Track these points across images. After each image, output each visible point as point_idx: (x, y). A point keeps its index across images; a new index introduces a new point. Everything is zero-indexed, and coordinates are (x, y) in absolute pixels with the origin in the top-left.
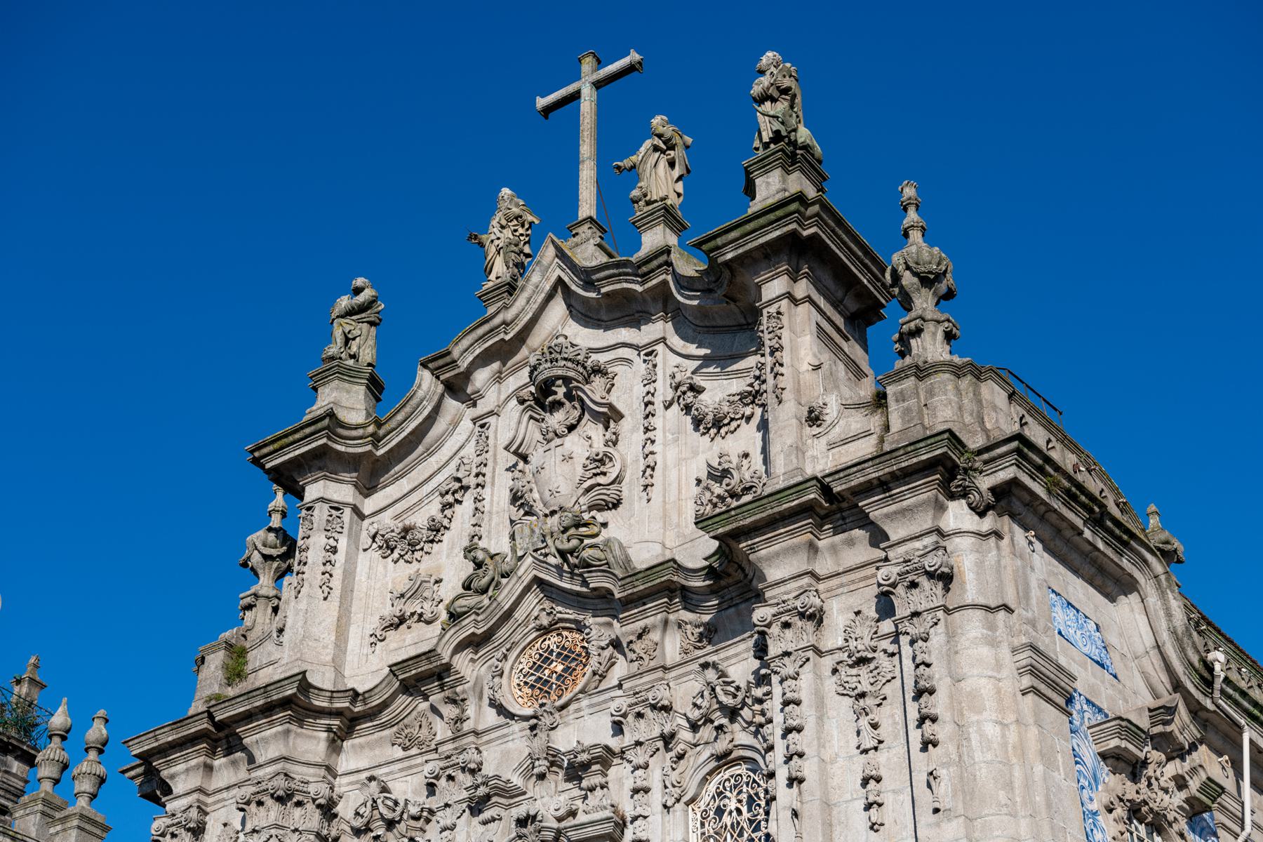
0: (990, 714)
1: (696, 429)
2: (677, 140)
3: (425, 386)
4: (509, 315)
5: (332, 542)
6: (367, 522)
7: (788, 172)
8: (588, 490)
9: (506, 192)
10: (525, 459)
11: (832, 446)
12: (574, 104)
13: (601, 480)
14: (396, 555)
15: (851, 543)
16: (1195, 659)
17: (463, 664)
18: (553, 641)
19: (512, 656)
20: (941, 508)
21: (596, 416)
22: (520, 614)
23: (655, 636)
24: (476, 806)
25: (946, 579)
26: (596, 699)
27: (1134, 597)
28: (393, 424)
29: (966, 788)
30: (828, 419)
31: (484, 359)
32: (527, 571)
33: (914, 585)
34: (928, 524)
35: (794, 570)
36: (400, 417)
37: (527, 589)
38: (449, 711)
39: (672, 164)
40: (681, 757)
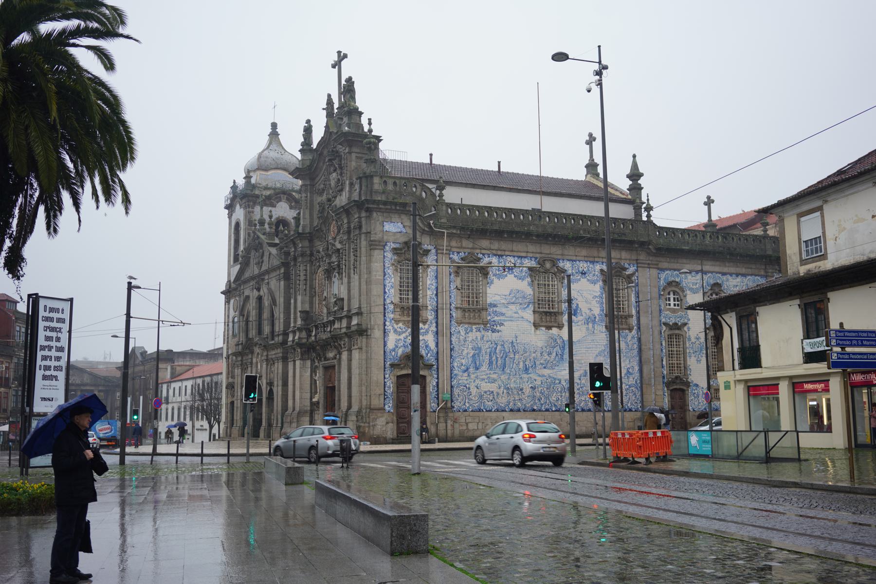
25: (360, 227)
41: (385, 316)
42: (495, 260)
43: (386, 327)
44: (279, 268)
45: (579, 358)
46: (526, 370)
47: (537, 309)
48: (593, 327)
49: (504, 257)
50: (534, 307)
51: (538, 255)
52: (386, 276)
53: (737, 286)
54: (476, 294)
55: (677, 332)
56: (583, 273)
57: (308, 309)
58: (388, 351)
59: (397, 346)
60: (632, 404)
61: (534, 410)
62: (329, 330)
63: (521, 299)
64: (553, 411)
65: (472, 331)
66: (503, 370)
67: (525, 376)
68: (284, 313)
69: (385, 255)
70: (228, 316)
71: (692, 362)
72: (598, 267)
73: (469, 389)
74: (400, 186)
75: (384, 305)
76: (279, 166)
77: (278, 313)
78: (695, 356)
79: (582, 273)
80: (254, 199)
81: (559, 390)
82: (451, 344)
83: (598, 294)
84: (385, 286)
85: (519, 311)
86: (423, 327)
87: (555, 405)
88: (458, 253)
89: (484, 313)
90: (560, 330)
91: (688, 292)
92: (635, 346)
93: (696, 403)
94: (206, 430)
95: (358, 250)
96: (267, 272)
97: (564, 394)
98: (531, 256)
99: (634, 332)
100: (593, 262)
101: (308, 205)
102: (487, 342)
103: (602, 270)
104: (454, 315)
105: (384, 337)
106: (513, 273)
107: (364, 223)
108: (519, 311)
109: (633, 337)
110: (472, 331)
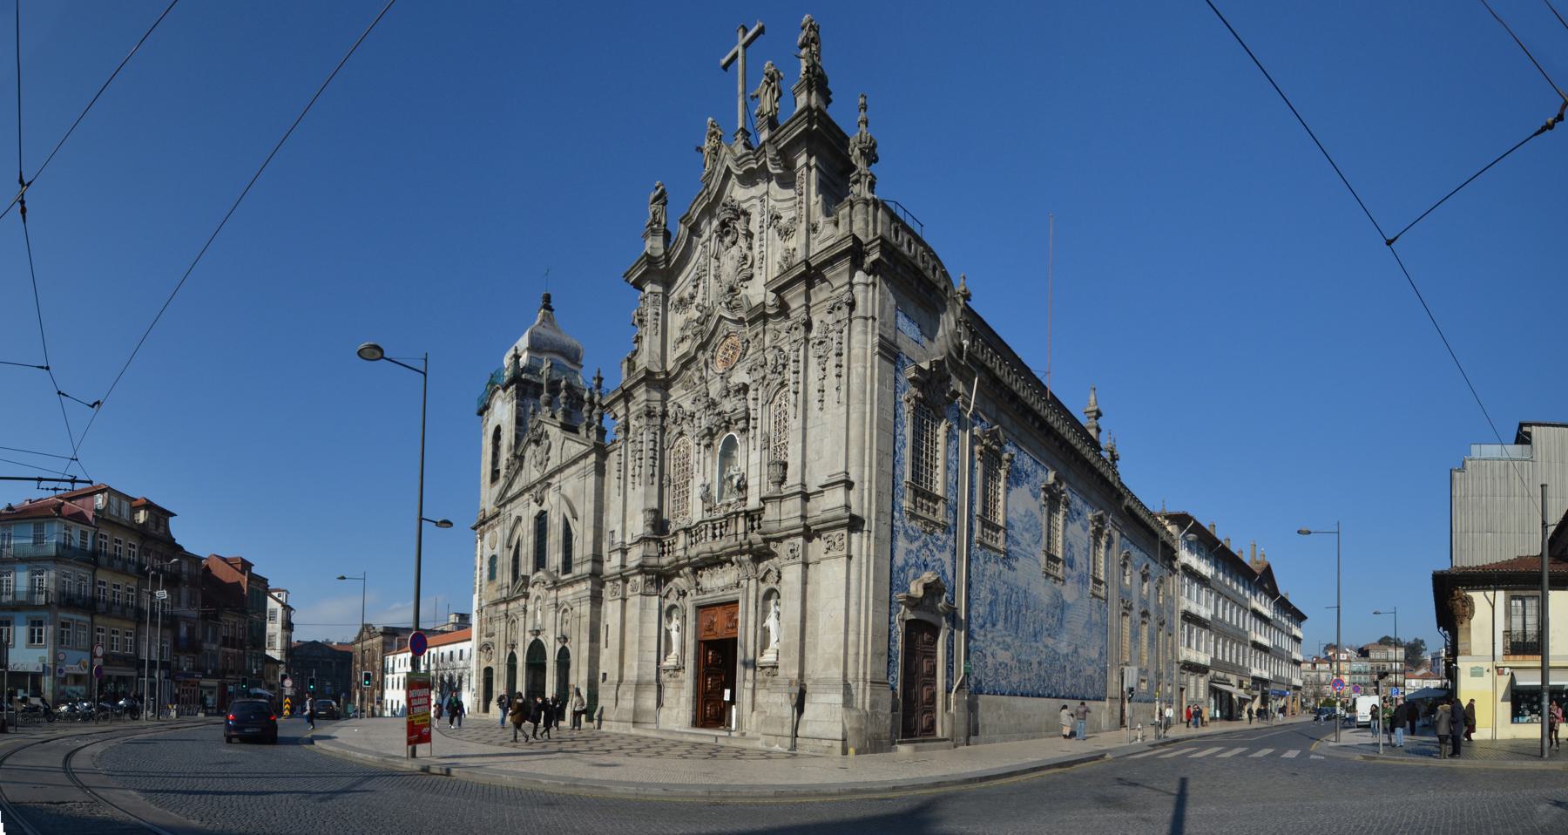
41: (893, 499)
46: (1035, 636)
58: (895, 569)
59: (907, 563)
61: (1039, 696)
62: (733, 531)
66: (1017, 630)
67: (1034, 644)
73: (985, 656)
83: (1086, 546)
85: (1033, 545)
86: (941, 536)
105: (892, 541)
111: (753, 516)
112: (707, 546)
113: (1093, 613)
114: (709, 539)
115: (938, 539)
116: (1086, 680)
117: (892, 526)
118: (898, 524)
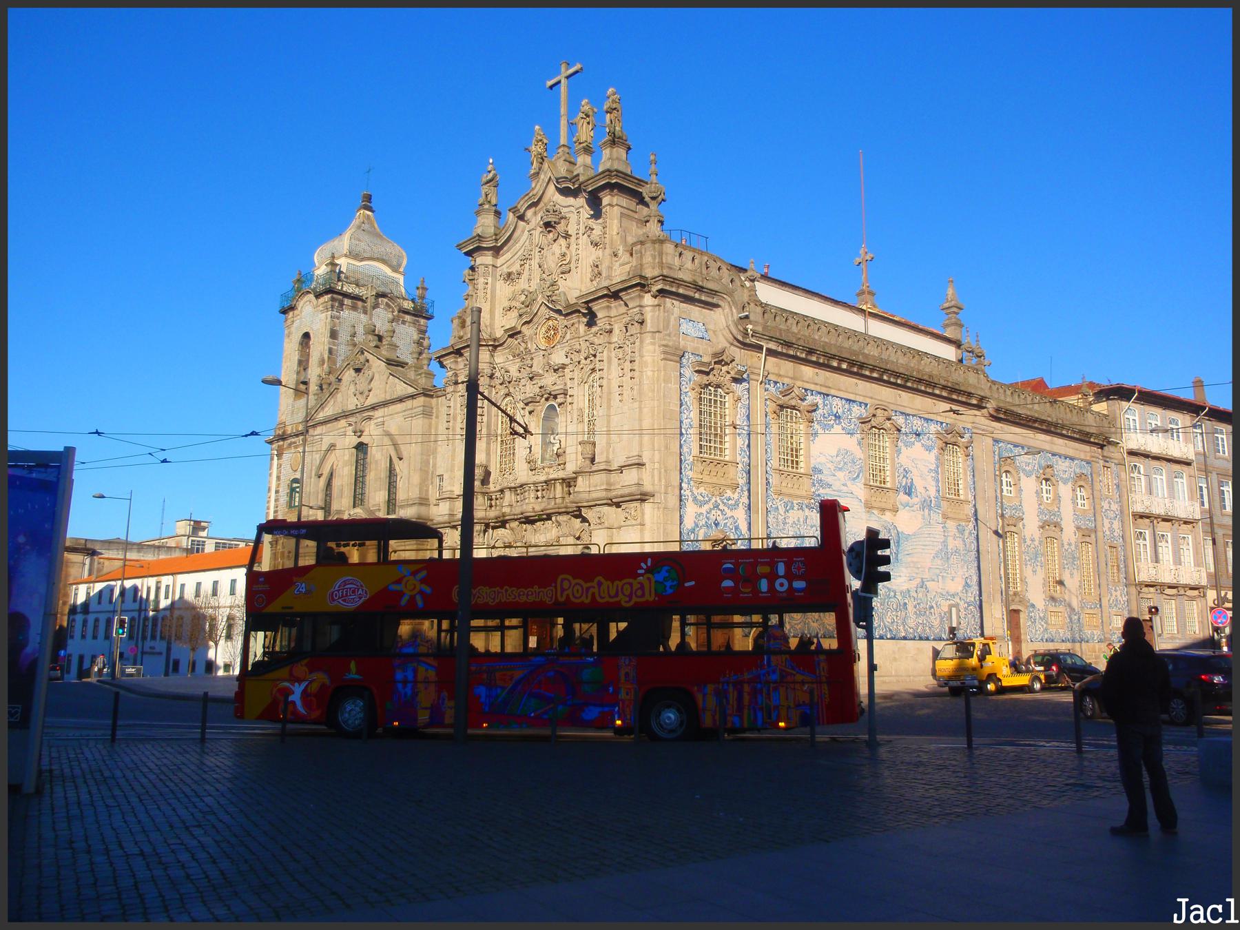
0: (650, 368)
1: (591, 245)
2: (591, 113)
3: (510, 220)
4: (535, 192)
5: (486, 281)
6: (498, 269)
7: (614, 148)
8: (561, 265)
9: (537, 127)
10: (543, 249)
11: (620, 265)
12: (559, 85)
13: (564, 262)
14: (508, 283)
15: (620, 305)
16: (742, 329)
17: (525, 329)
18: (550, 323)
19: (539, 329)
20: (641, 297)
21: (563, 236)
22: (539, 314)
23: (576, 325)
24: (531, 379)
25: (642, 323)
26: (562, 346)
27: (719, 309)
28: (501, 234)
29: (640, 393)
30: (620, 255)
31: (529, 207)
32: (540, 299)
33: (632, 324)
34: (638, 304)
35: (604, 316)
36: (503, 232)
37: (541, 306)
38: (523, 344)
39: (588, 123)
40: (582, 368)
41: (681, 473)
42: (819, 399)
43: (682, 492)
44: (412, 397)
45: (915, 560)
47: (867, 482)
48: (929, 515)
49: (830, 397)
50: (866, 479)
51: (868, 401)
52: (683, 407)
53: (1066, 471)
54: (797, 451)
55: (1013, 528)
56: (918, 435)
57: (484, 463)
59: (697, 525)
60: (971, 631)
63: (850, 464)
64: (888, 639)
65: (793, 509)
68: (421, 469)
69: (682, 372)
70: (278, 478)
71: (1028, 571)
72: (933, 428)
74: (701, 264)
75: (681, 455)
76: (376, 256)
77: (406, 472)
78: (1031, 565)
79: (916, 434)
80: (340, 297)
81: (895, 606)
82: (768, 527)
83: (933, 467)
84: (681, 422)
85: (849, 483)
86: (732, 496)
87: (890, 630)
88: (776, 383)
89: (805, 480)
90: (895, 515)
91: (1022, 474)
92: (974, 546)
93: (1034, 631)
94: (160, 653)
95: (637, 359)
96: (385, 404)
97: (899, 613)
98: (861, 401)
99: (971, 525)
100: (927, 420)
101: (489, 296)
102: (812, 527)
103: (938, 433)
104: (770, 481)
105: (681, 508)
106: (840, 423)
107: (649, 316)
108: (849, 483)
109: (970, 533)
110: (793, 509)
111: (569, 483)
112: (532, 504)
113: (950, 539)
114: (532, 500)
115: (729, 499)
116: (942, 618)
117: (681, 496)
118: (688, 493)
